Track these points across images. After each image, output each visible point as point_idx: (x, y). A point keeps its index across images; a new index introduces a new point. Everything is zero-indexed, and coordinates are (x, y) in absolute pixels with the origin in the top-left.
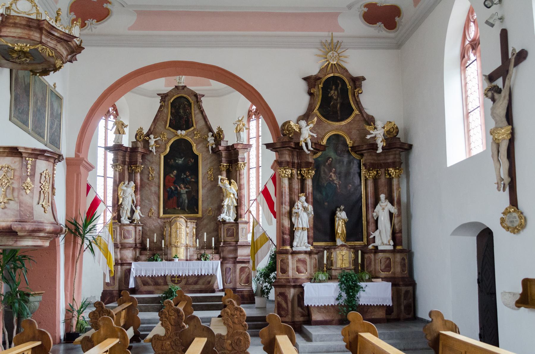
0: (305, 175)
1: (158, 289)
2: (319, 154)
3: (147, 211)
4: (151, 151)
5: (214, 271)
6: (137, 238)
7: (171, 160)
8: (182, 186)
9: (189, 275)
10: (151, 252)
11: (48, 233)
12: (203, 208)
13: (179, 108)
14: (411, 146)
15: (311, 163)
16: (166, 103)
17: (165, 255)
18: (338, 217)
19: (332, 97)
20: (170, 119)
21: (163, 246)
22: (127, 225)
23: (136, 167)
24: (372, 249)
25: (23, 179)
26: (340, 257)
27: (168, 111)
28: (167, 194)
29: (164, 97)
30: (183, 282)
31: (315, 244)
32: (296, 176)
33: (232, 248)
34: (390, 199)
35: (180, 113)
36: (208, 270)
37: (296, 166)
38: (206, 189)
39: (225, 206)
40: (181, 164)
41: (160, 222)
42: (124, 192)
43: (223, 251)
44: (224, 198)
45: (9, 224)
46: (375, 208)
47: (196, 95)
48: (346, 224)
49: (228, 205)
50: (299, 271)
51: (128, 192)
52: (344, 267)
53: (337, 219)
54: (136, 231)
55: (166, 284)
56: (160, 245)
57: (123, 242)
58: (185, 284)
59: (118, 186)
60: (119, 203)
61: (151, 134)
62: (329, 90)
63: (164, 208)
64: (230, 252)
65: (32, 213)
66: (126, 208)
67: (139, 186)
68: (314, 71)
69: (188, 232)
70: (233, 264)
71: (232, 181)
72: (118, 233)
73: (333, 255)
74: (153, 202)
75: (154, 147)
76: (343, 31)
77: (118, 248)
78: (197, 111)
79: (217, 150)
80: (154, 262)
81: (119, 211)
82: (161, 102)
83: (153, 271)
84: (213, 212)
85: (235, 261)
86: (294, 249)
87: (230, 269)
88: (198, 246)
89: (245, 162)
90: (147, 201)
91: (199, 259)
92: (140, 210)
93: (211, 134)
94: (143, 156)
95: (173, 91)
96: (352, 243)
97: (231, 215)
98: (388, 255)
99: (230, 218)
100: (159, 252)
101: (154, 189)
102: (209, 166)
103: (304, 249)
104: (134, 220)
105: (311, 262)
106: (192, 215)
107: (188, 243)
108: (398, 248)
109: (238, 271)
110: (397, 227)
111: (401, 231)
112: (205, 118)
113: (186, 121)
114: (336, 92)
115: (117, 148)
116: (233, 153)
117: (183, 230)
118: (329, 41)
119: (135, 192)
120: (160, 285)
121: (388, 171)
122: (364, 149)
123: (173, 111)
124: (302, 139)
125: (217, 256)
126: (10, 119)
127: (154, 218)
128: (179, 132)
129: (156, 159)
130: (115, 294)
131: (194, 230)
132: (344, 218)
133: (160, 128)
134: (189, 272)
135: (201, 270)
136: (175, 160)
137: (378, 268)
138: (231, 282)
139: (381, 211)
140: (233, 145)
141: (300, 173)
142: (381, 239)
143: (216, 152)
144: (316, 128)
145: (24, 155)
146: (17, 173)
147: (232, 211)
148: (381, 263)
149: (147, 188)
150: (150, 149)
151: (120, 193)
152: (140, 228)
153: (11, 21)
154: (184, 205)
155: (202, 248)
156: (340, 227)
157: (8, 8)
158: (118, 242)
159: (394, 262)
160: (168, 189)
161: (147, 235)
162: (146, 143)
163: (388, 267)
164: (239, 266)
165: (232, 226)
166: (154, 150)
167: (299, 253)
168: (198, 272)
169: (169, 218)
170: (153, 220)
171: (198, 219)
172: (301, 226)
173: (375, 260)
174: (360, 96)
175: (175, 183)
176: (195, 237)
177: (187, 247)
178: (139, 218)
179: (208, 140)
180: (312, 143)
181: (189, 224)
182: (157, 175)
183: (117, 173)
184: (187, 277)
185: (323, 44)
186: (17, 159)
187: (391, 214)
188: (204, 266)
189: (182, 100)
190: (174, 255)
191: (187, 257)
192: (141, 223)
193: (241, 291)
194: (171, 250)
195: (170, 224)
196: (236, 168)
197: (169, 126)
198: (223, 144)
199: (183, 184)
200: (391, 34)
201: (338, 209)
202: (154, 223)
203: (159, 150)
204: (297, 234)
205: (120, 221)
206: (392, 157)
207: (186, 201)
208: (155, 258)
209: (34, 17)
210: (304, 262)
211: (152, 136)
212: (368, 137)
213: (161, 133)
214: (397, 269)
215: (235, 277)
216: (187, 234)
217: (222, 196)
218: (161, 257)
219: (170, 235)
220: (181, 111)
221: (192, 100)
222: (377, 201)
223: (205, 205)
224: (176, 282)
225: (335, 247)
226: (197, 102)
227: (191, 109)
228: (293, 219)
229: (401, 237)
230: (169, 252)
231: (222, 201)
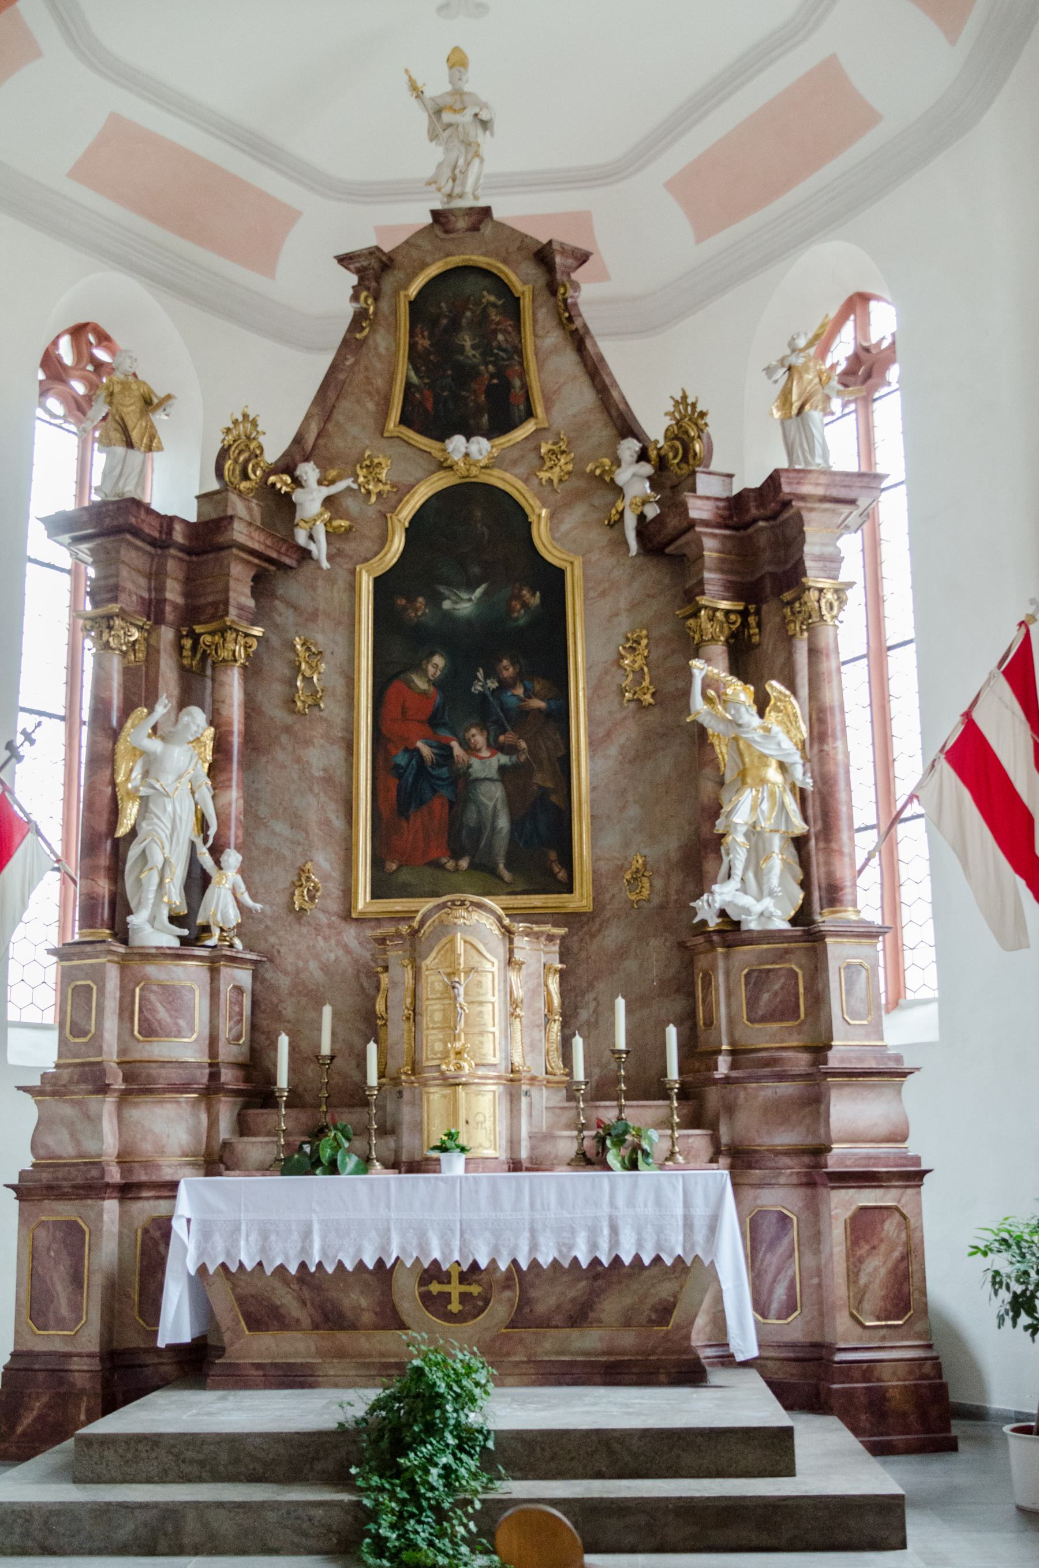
1: (341, 1354)
3: (284, 878)
4: (305, 555)
5: (700, 1236)
6: (225, 1030)
7: (411, 600)
8: (478, 738)
9: (535, 1264)
10: (304, 1117)
12: (596, 859)
13: (455, 325)
16: (385, 305)
17: (384, 1131)
20: (408, 386)
21: (373, 1079)
23: (223, 631)
27: (393, 347)
28: (393, 783)
29: (372, 269)
30: (500, 1310)
33: (786, 1089)
35: (462, 349)
36: (660, 1230)
38: (613, 750)
40: (472, 619)
41: (353, 944)
42: (151, 766)
43: (730, 1109)
44: (724, 797)
47: (543, 255)
49: (753, 832)
51: (175, 770)
54: (214, 995)
55: (392, 1319)
56: (356, 1076)
57: (136, 1056)
58: (512, 1324)
59: (115, 735)
60: (121, 831)
61: (306, 459)
63: (377, 863)
64: (778, 1113)
66: (157, 858)
67: (236, 741)
69: (519, 993)
70: (801, 1192)
71: (775, 687)
72: (112, 1005)
74: (315, 829)
77: (103, 1089)
78: (553, 338)
79: (673, 523)
80: (320, 1180)
81: (116, 872)
82: (355, 298)
83: (307, 1235)
84: (659, 883)
85: (816, 1171)
87: (784, 1219)
88: (580, 1075)
89: (843, 578)
90: (281, 827)
91: (590, 1160)
92: (242, 871)
94: (262, 584)
95: (420, 242)
97: (774, 880)
99: (768, 903)
100: (347, 1118)
101: (321, 757)
102: (624, 623)
104: (206, 929)
106: (537, 900)
107: (517, 1060)
109: (837, 1235)
112: (595, 371)
113: (490, 390)
115: (115, 525)
116: (763, 540)
117: (487, 980)
119: (213, 771)
120: (354, 1327)
123: (424, 343)
125: (697, 1139)
127: (323, 919)
128: (457, 444)
129: (334, 596)
130: (81, 1381)
133: (354, 431)
134: (534, 1247)
135: (614, 1230)
136: (435, 599)
138: (790, 1307)
140: (774, 480)
143: (664, 543)
147: (779, 863)
149: (281, 756)
150: (301, 537)
151: (129, 775)
152: (244, 977)
154: (490, 845)
155: (602, 1089)
158: (110, 1054)
160: (401, 759)
161: (278, 1017)
162: (281, 508)
164: (842, 1204)
165: (782, 956)
166: (320, 549)
168: (594, 1246)
169: (406, 917)
170: (318, 929)
171: (569, 919)
175: (435, 721)
176: (556, 1027)
177: (513, 1083)
178: (233, 917)
179: (622, 477)
182: (339, 684)
183: (115, 665)
184: (522, 1279)
188: (631, 1203)
189: (471, 285)
190: (437, 1136)
191: (513, 1143)
192: (248, 948)
193: (867, 1370)
194: (417, 1103)
195: (414, 943)
196: (784, 623)
197: (404, 421)
198: (707, 485)
199: (483, 727)
202: (321, 950)
203: (349, 547)
205: (122, 935)
207: (503, 823)
208: (326, 1154)
211: (309, 472)
213: (360, 460)
215: (819, 1272)
216: (515, 1004)
217: (707, 787)
218: (359, 1143)
219: (414, 1014)
220: (467, 341)
221: (522, 279)
223: (611, 840)
224: (455, 1307)
226: (552, 287)
230: (407, 1114)
231: (715, 810)
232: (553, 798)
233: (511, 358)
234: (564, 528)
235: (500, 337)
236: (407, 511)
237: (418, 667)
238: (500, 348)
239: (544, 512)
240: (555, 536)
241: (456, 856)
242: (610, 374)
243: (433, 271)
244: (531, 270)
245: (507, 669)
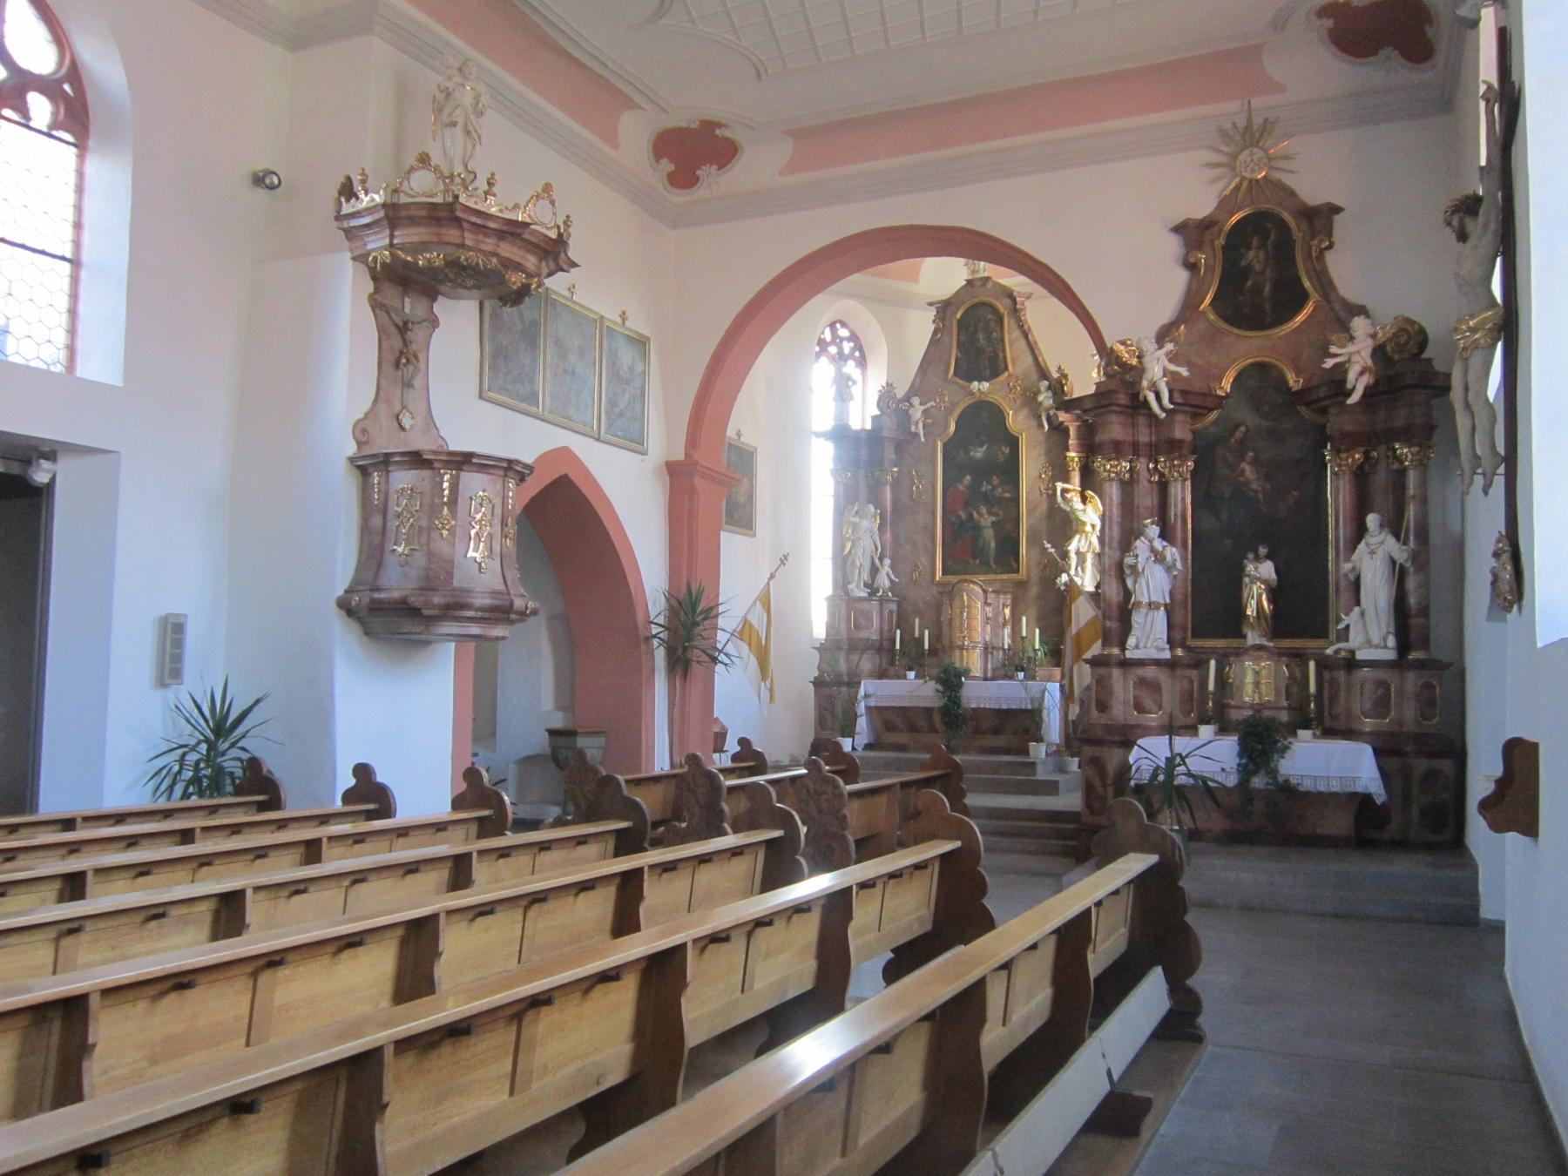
0: (1166, 472)
2: (1214, 415)
8: (984, 510)
11: (482, 609)
15: (1181, 442)
19: (1249, 267)
22: (861, 599)
25: (434, 511)
26: (1249, 679)
32: (1144, 474)
39: (1073, 556)
45: (404, 593)
46: (1354, 548)
48: (1274, 593)
50: (1140, 708)
52: (1257, 701)
53: (1247, 580)
65: (450, 574)
68: (1202, 205)
73: (1232, 671)
75: (921, 426)
76: (1281, 88)
78: (1017, 333)
86: (1129, 655)
92: (893, 567)
96: (1287, 643)
98: (1382, 674)
103: (1154, 654)
105: (1171, 688)
110: (1412, 600)
112: (1032, 348)
114: (1262, 254)
115: (841, 434)
118: (1241, 122)
123: (963, 338)
124: (1145, 383)
126: (481, 397)
131: (1007, 611)
136: (967, 452)
137: (1356, 707)
139: (1367, 558)
145: (436, 465)
146: (427, 501)
150: (913, 429)
152: (894, 607)
153: (403, 214)
156: (1256, 599)
157: (396, 191)
160: (953, 519)
163: (1382, 705)
167: (1141, 663)
172: (1145, 600)
174: (1330, 257)
175: (967, 504)
178: (887, 583)
180: (1171, 392)
181: (991, 598)
185: (1224, 135)
186: (427, 473)
191: (985, 671)
197: (955, 374)
200: (1422, 76)
201: (1251, 556)
204: (1137, 618)
207: (993, 545)
209: (439, 200)
210: (1154, 687)
211: (916, 401)
214: (1407, 713)
221: (1002, 306)
222: (1360, 531)
225: (1240, 653)
228: (1129, 582)
236: (956, 414)
237: (960, 480)
240: (1016, 420)
241: (975, 557)
243: (968, 305)
244: (1008, 301)
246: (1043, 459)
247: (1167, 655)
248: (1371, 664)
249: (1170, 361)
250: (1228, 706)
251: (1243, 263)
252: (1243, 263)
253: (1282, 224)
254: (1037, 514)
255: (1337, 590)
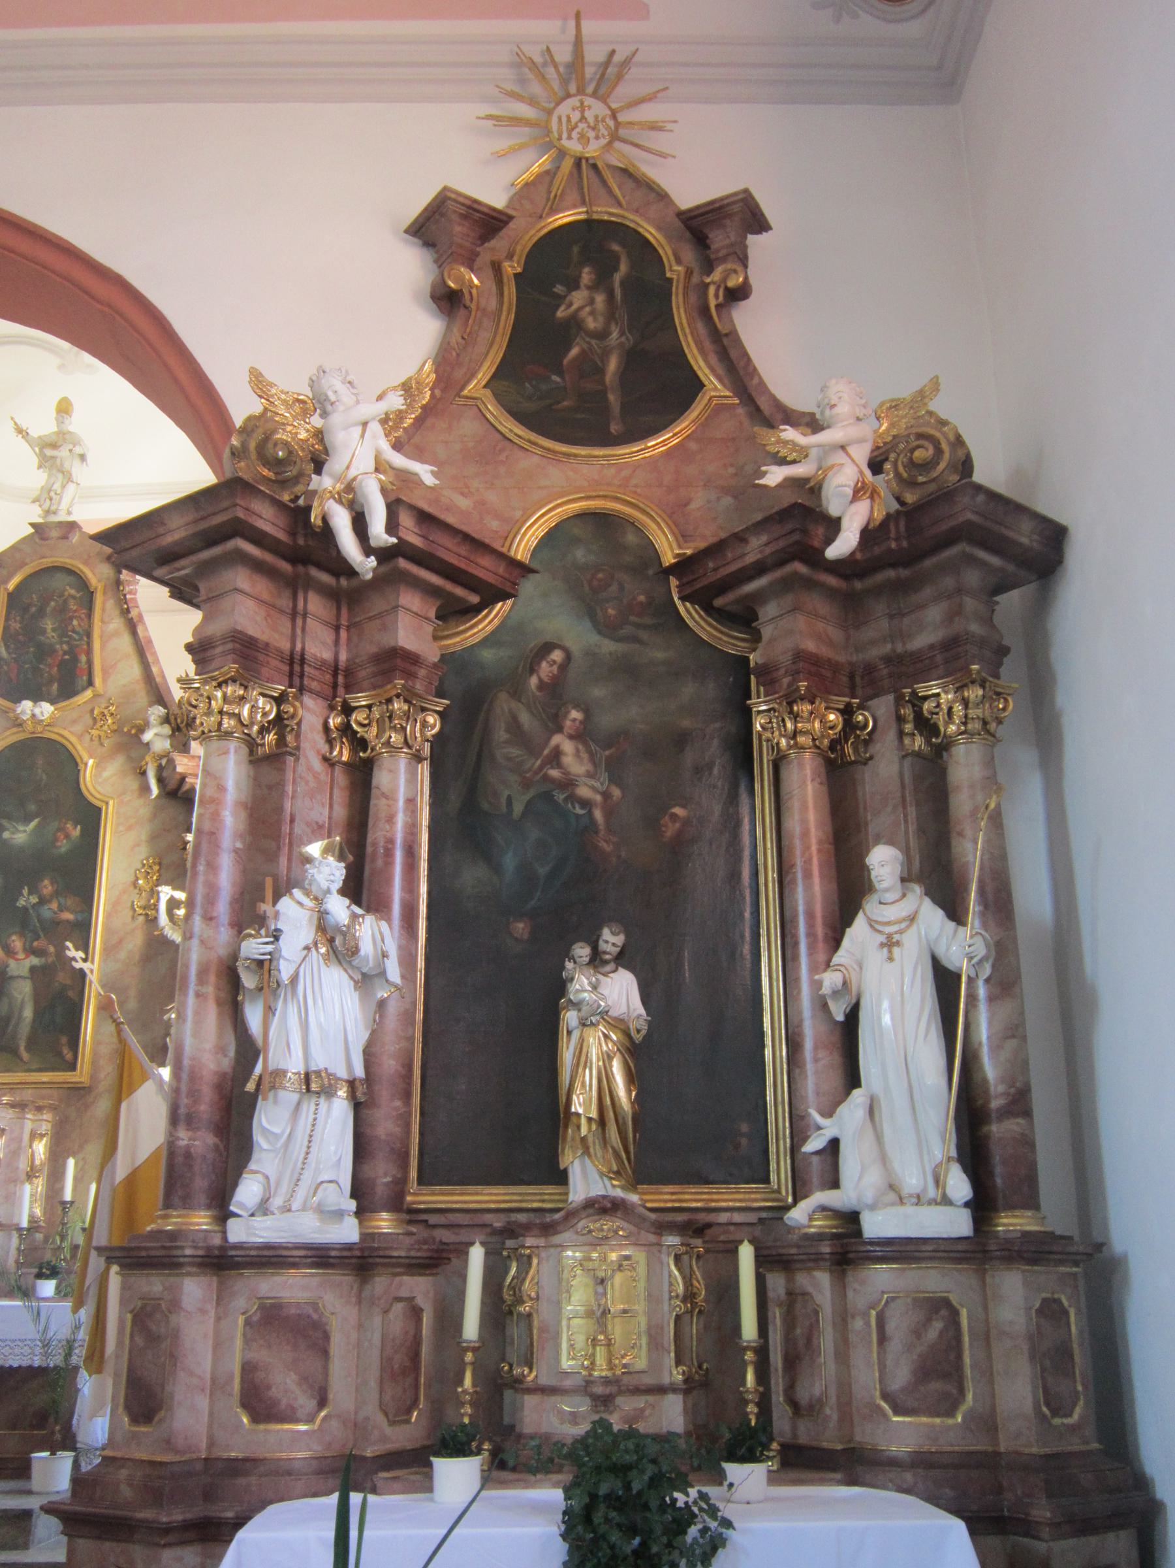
8: (17, 943)
13: (41, 612)
14: (1055, 536)
15: (412, 659)
18: (577, 1005)
19: (574, 324)
24: (820, 1237)
31: (421, 1197)
32: (312, 742)
34: (940, 881)
35: (44, 632)
37: (315, 679)
46: (835, 941)
48: (640, 1054)
52: (601, 1370)
53: (570, 1018)
62: (559, 289)
73: (538, 1278)
78: (117, 623)
86: (238, 1232)
93: (161, 711)
98: (934, 1280)
103: (308, 1228)
105: (359, 1334)
108: (1010, 1223)
110: (990, 1069)
111: (1020, 1103)
114: (600, 299)
121: (917, 701)
122: (750, 559)
123: (16, 626)
128: (26, 706)
131: (41, 1148)
132: (619, 1010)
137: (866, 1379)
139: (875, 958)
141: (346, 729)
142: (884, 1159)
144: (475, 484)
148: (883, 1339)
159: (985, 1337)
163: (940, 1374)
167: (270, 1258)
172: (294, 1065)
173: (843, 1318)
180: (393, 508)
187: (945, 982)
189: (59, 581)
199: (22, 935)
201: (582, 951)
204: (270, 1120)
206: (934, 613)
210: (306, 1332)
212: (774, 476)
220: (49, 625)
227: (90, 616)
228: (253, 1016)
229: (1027, 1142)
232: (70, 994)
233: (81, 639)
234: (106, 774)
235: (75, 622)
238: (74, 631)
239: (91, 762)
240: (101, 777)
242: (154, 654)
245: (47, 887)
246: (143, 852)
247: (348, 1231)
248: (903, 1251)
249: (397, 446)
250: (517, 1383)
251: (561, 313)
252: (561, 313)
253: (643, 248)
254: (123, 955)
255: (794, 1044)
